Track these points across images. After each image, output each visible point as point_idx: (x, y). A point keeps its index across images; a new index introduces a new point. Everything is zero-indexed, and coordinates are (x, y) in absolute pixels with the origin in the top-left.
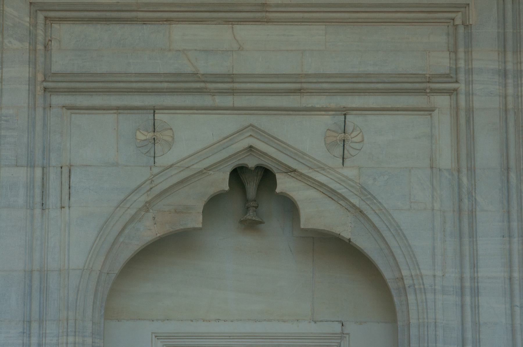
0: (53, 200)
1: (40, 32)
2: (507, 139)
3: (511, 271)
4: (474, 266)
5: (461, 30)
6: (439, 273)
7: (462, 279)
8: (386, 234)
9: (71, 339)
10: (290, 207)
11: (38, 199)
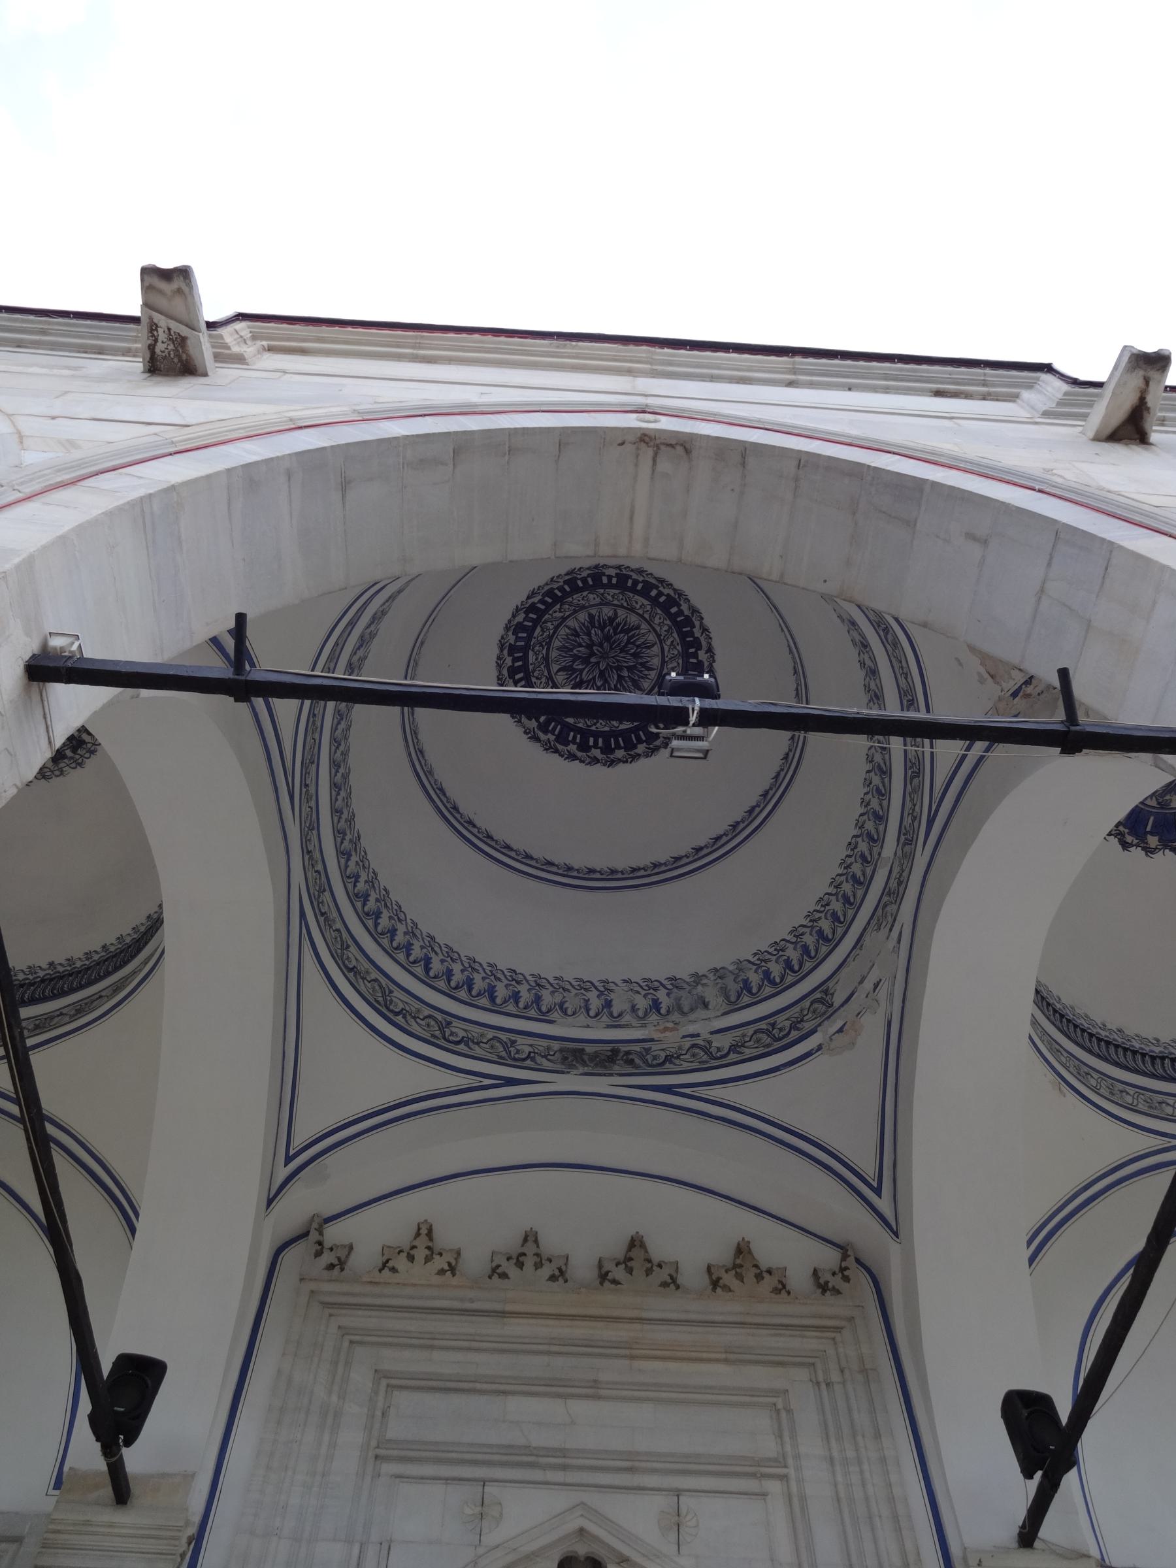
1: (381, 1398)
2: (844, 1532)
5: (783, 1414)
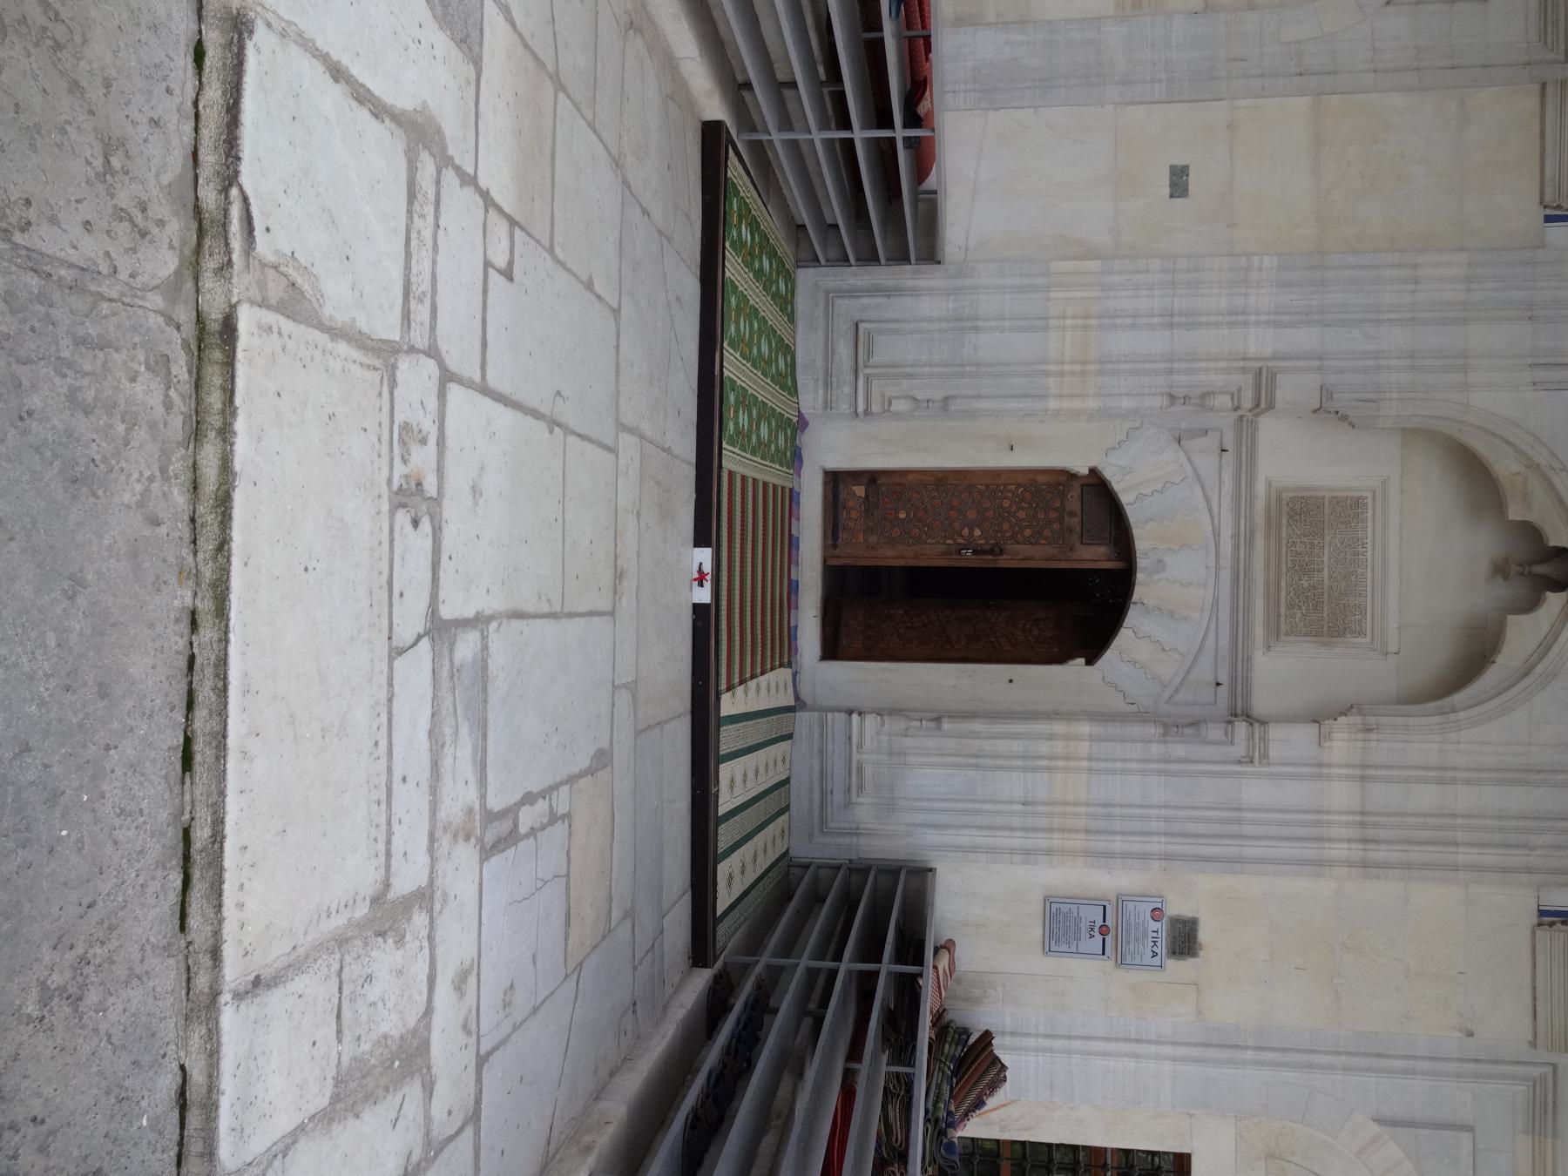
0: (1541, 374)
3: (1462, 816)
4: (1468, 782)
6: (1461, 747)
7: (1454, 769)
8: (1504, 697)
9: (1395, 395)
10: (1531, 604)
11: (1541, 361)
